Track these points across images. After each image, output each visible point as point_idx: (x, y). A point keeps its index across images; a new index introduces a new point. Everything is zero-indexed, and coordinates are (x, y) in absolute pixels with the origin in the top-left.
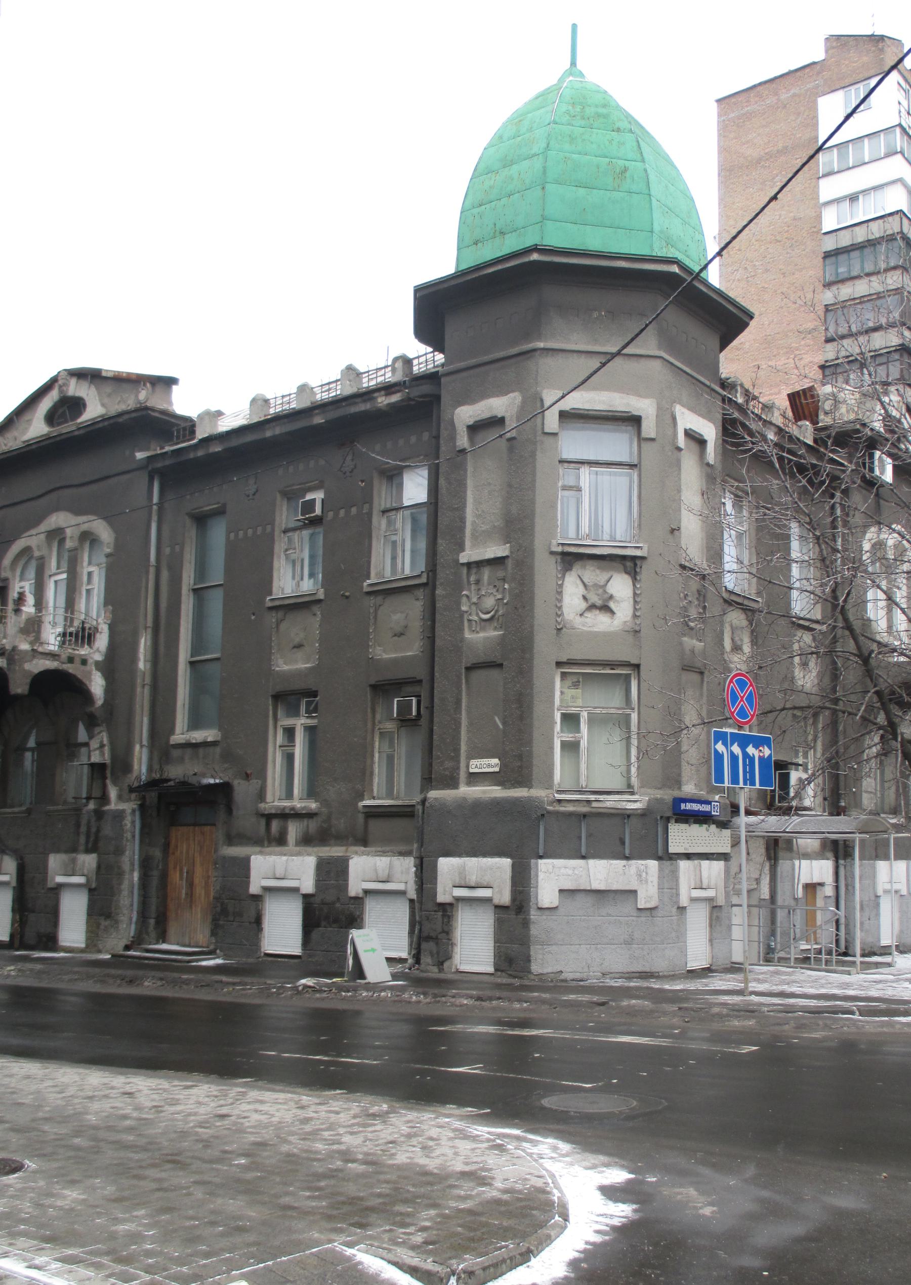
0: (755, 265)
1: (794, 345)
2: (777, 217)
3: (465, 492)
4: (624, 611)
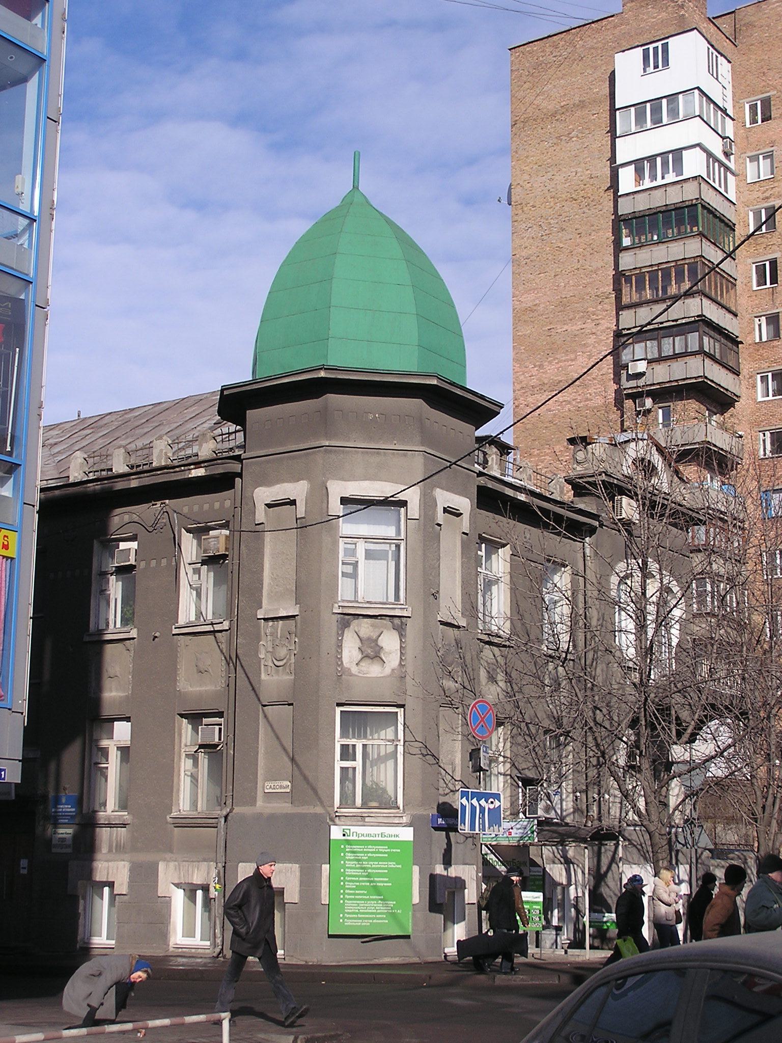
0: (550, 224)
1: (591, 309)
3: (262, 559)
4: (392, 660)
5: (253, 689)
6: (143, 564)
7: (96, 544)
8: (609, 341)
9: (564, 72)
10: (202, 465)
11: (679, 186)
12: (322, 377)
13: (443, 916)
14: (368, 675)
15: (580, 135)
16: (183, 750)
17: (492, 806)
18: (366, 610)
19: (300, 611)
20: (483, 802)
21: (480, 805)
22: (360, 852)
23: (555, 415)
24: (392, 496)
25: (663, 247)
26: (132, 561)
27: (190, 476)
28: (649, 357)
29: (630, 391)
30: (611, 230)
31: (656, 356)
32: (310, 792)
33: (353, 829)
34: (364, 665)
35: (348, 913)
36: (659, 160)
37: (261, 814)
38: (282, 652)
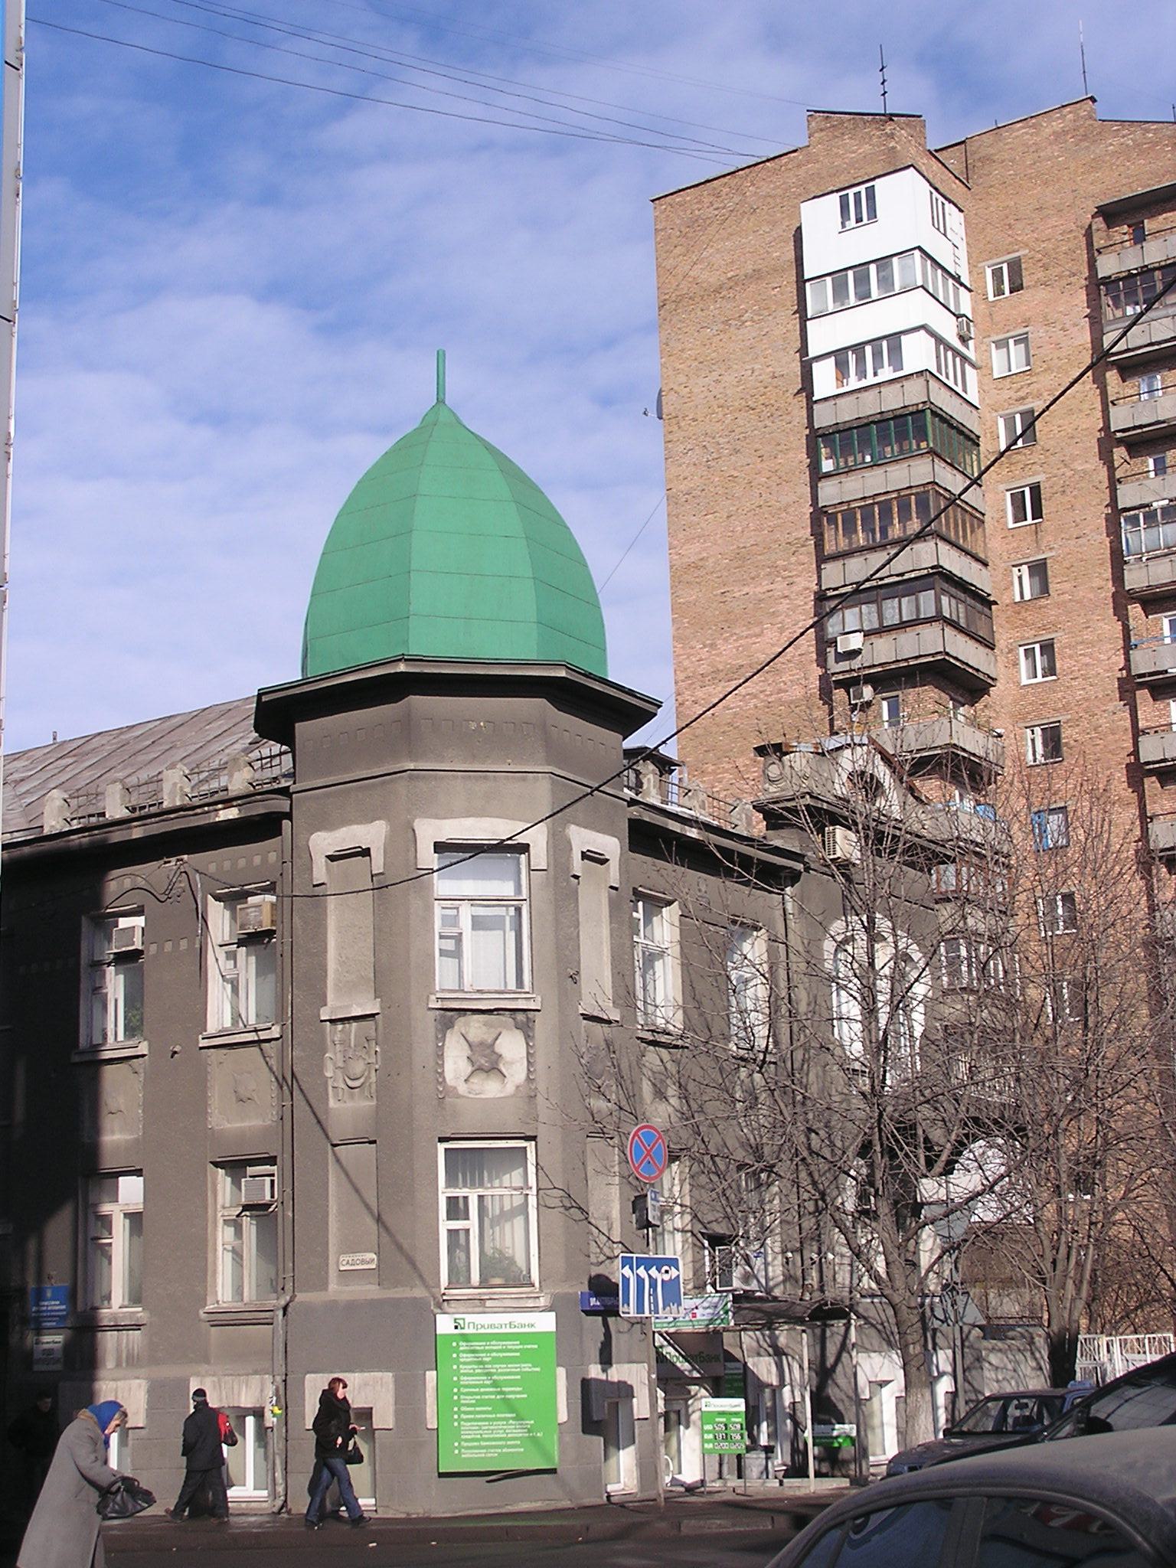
2: (750, 372)
4: (516, 1073)
5: (319, 1122)
6: (153, 948)
7: (84, 921)
8: (807, 607)
9: (730, 230)
10: (235, 803)
11: (898, 385)
12: (402, 673)
13: (602, 1439)
14: (483, 1096)
15: (756, 318)
16: (220, 1214)
17: (666, 1277)
18: (475, 1002)
19: (382, 1008)
20: (653, 1272)
21: (650, 1276)
22: (483, 1351)
23: (736, 714)
24: (510, 839)
25: (879, 471)
26: (138, 945)
27: (217, 819)
28: (866, 628)
29: (841, 677)
30: (804, 450)
31: (876, 626)
32: (408, 1267)
33: (469, 1318)
35: (466, 1440)
36: (868, 349)
37: (335, 1301)
38: (358, 1067)
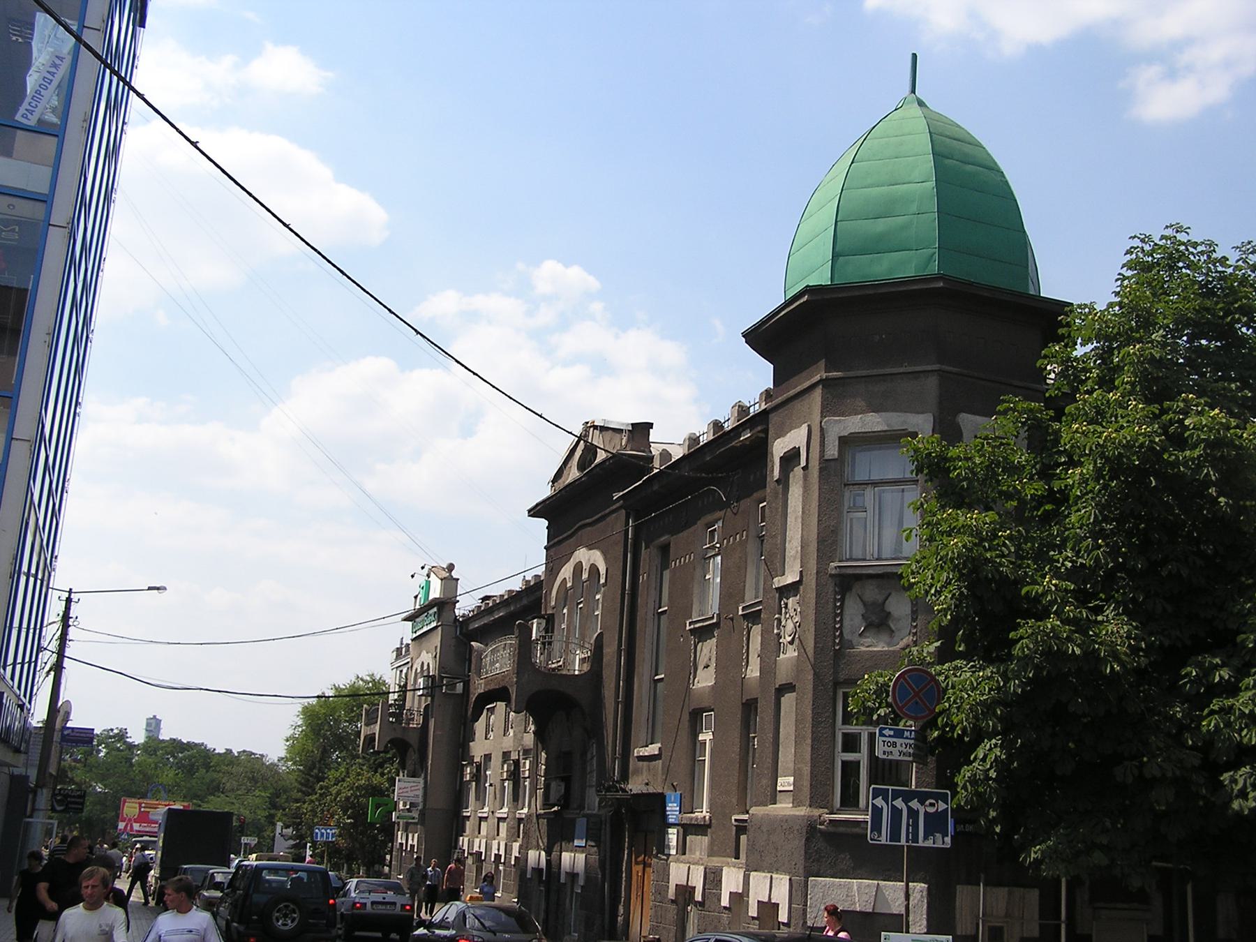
17: (931, 810)
20: (914, 804)
21: (909, 808)
34: (868, 635)
